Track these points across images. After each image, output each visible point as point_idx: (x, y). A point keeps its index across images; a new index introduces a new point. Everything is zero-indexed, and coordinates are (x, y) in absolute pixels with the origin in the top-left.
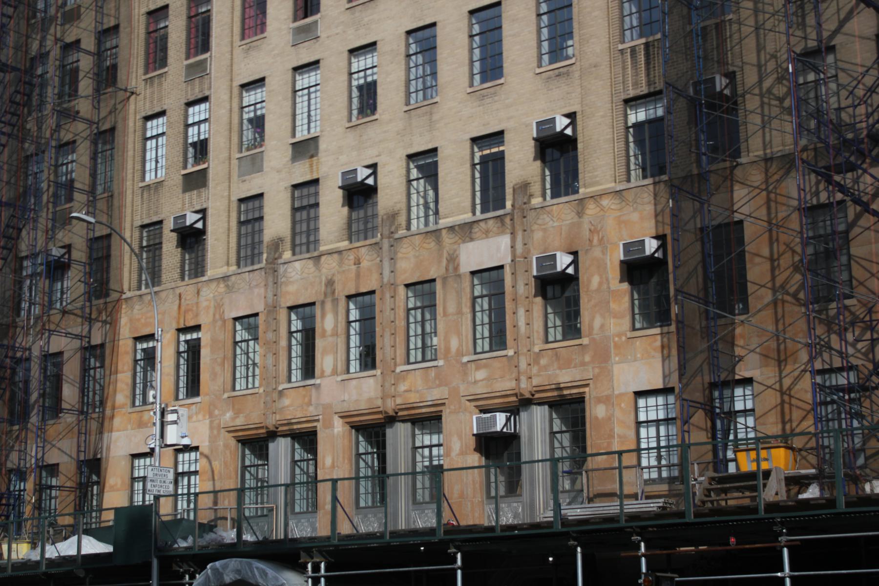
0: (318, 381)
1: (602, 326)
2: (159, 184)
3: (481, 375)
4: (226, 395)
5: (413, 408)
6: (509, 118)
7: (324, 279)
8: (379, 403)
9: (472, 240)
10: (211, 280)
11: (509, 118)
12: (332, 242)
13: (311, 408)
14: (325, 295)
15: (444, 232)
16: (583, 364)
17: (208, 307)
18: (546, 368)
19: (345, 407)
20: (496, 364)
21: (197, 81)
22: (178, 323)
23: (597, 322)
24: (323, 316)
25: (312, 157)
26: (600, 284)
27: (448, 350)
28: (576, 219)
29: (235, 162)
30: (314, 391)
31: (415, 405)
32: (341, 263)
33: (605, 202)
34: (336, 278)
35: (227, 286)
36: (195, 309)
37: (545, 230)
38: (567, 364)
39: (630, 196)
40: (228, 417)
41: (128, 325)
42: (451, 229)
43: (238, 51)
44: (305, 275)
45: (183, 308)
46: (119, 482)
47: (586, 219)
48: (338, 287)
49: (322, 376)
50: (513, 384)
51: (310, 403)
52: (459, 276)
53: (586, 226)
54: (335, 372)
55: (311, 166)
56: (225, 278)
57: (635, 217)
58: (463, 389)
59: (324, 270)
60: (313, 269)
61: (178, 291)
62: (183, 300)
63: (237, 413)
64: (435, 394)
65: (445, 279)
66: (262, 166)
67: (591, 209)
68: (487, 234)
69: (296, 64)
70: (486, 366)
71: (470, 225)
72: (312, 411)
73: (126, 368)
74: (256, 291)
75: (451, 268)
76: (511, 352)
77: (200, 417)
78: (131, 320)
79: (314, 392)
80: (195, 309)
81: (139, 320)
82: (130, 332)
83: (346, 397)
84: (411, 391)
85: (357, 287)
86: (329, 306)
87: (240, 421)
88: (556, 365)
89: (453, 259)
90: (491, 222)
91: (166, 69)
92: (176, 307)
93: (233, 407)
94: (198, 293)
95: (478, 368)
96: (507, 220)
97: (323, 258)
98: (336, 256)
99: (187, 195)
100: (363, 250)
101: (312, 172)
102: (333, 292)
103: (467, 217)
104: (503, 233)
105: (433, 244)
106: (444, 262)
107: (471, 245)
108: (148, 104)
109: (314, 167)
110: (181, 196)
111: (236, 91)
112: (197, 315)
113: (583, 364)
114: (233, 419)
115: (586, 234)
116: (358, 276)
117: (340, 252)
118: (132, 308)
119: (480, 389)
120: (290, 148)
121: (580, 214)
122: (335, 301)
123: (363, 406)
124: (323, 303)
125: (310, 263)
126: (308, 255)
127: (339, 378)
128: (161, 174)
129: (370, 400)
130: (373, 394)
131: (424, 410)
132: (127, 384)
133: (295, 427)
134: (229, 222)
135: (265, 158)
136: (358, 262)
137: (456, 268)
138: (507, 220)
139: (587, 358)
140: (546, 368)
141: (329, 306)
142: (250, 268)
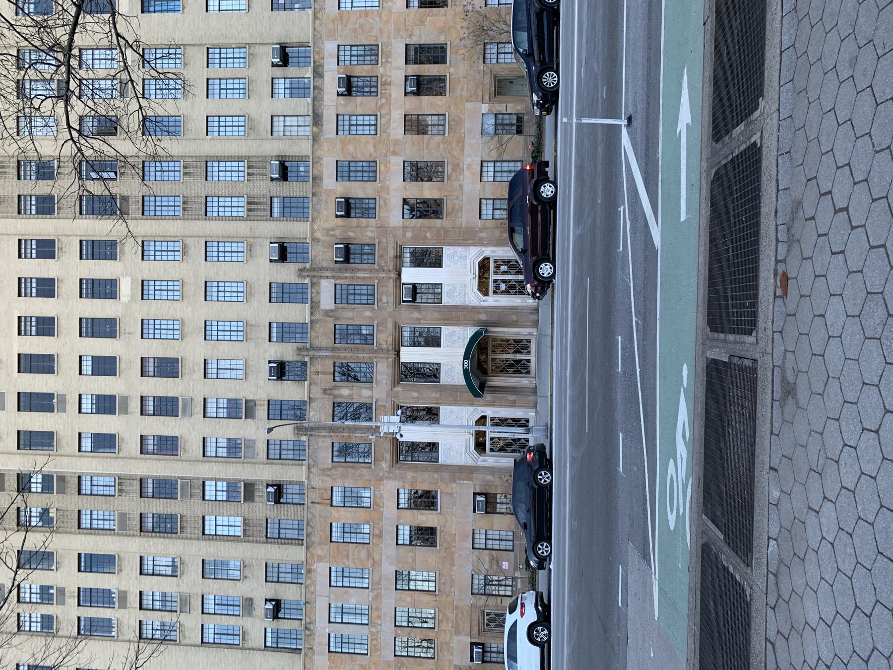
0: (374, 400)
1: (371, 232)
2: (245, 521)
3: (384, 299)
6: (265, 279)
9: (319, 302)
10: (308, 478)
11: (265, 279)
12: (304, 392)
13: (387, 406)
14: (331, 394)
15: (313, 318)
16: (387, 243)
17: (323, 481)
18: (386, 262)
19: (389, 383)
20: (381, 289)
21: (193, 491)
22: (327, 504)
23: (369, 234)
24: (341, 396)
25: (255, 404)
26: (352, 231)
27: (371, 317)
28: (321, 243)
29: (246, 460)
30: (379, 403)
32: (316, 384)
33: (316, 227)
34: (323, 387)
35: (314, 466)
36: (322, 491)
37: (323, 260)
38: (386, 250)
39: (315, 214)
40: (385, 465)
41: (323, 546)
42: (312, 314)
43: (183, 457)
44: (318, 410)
45: (320, 501)
46: (411, 554)
47: (322, 238)
48: (328, 386)
49: (371, 397)
50: (391, 280)
51: (385, 406)
52: (336, 309)
54: (371, 389)
55: (260, 405)
56: (309, 468)
57: (325, 213)
58: (390, 309)
59: (318, 396)
60: (316, 403)
61: (310, 504)
62: (316, 501)
63: (383, 458)
65: (337, 318)
66: (252, 440)
67: (318, 235)
68: (318, 293)
69: (202, 415)
70: (381, 296)
71: (312, 307)
73: (347, 548)
74: (320, 444)
75: (331, 314)
76: (376, 281)
77: (382, 487)
78: (320, 544)
79: (379, 403)
80: (322, 491)
81: (321, 537)
82: (326, 545)
83: (385, 382)
85: (329, 373)
86: (336, 392)
87: (388, 456)
88: (385, 257)
89: (327, 313)
90: (313, 290)
91: (179, 515)
92: (318, 506)
93: (380, 461)
94: (313, 488)
95: (381, 300)
96: (314, 280)
97: (312, 396)
98: (312, 387)
99: (256, 499)
100: (312, 369)
101: (263, 405)
102: (330, 389)
103: (308, 306)
104: (319, 284)
105: (317, 325)
106: (327, 318)
107: (322, 303)
108: (196, 532)
109: (261, 403)
110: (256, 504)
111: (205, 459)
112: (326, 489)
113: (387, 243)
114: (386, 461)
115: (328, 238)
116: (324, 373)
117: (310, 384)
118: (313, 542)
119: (391, 300)
120: (249, 420)
121: (318, 241)
122: (335, 387)
123: (390, 371)
124: (335, 396)
125: (312, 404)
126: (308, 406)
127: (375, 386)
128: (239, 521)
129: (388, 367)
130: (385, 365)
132: (356, 547)
134: (278, 464)
135: (248, 437)
136: (317, 373)
137: (331, 311)
138: (314, 280)
139: (385, 240)
140: (386, 262)
141: (336, 392)
142: (307, 447)
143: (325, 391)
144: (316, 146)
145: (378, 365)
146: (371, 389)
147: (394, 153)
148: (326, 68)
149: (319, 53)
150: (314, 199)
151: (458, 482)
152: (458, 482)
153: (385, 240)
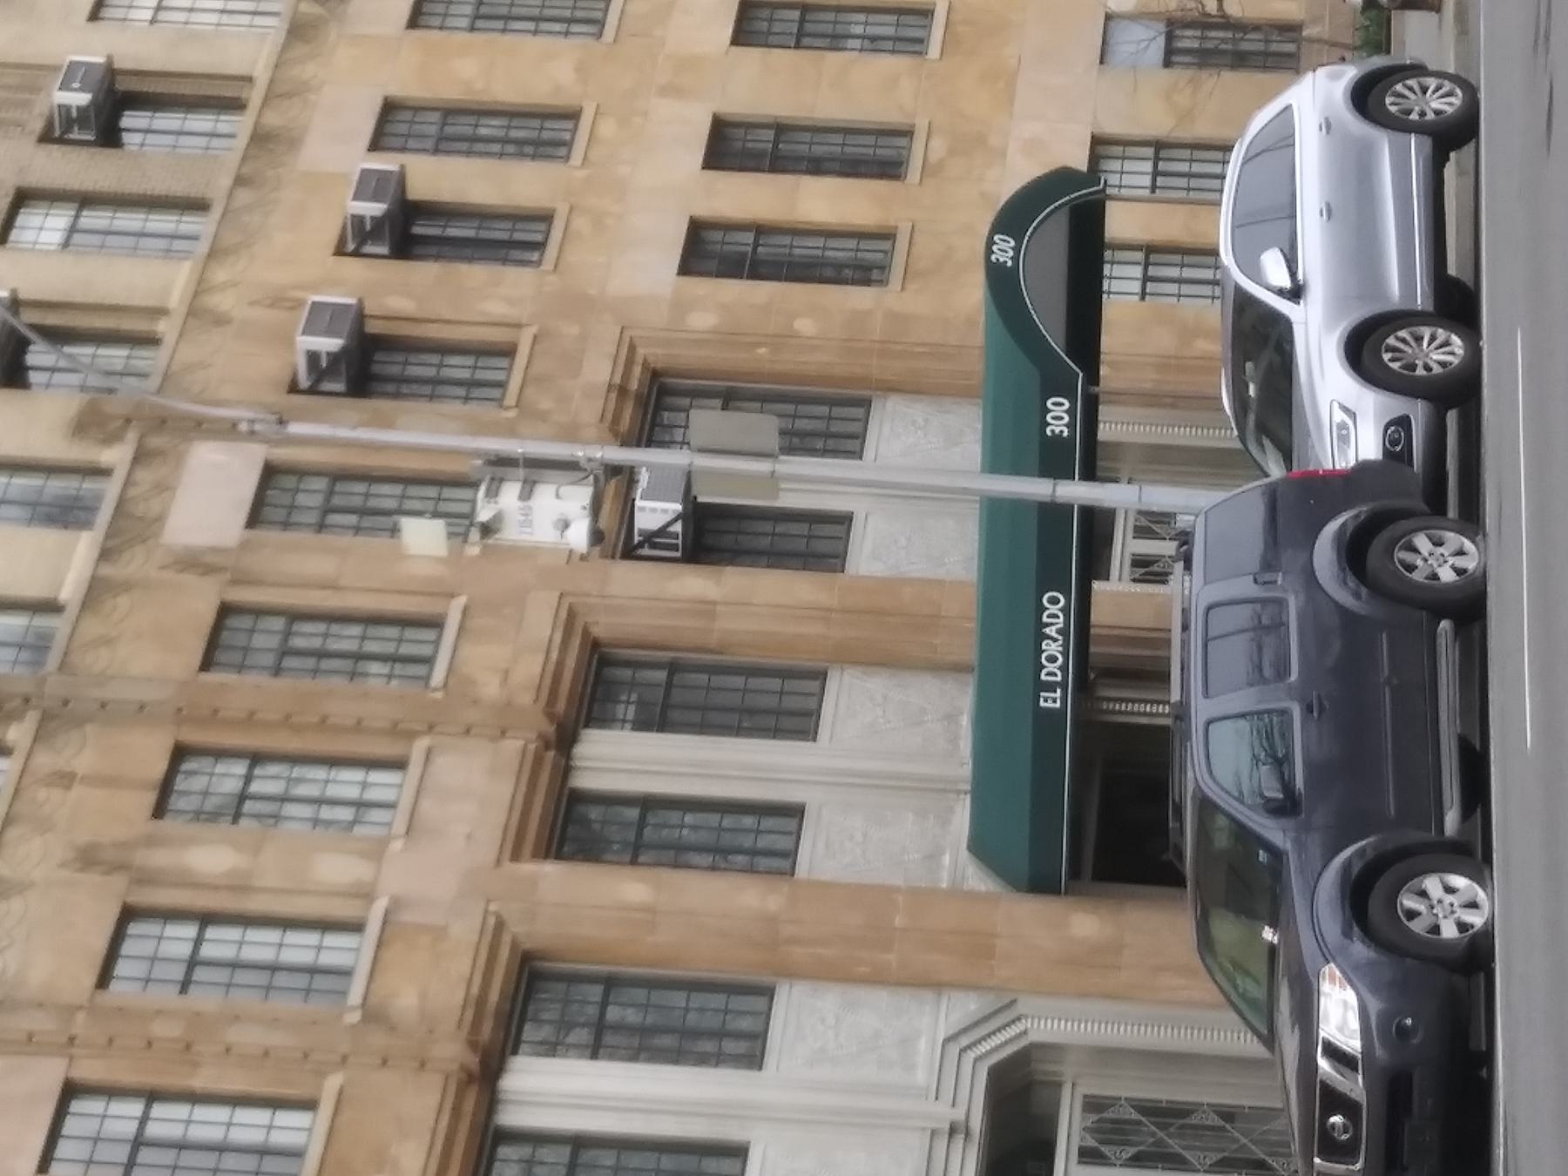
0: (380, 905)
7: (65, 874)
8: (512, 746)
9: (160, 519)
15: (107, 570)
30: (407, 917)
31: (551, 667)
32: (44, 826)
34: (83, 837)
51: (439, 933)
53: (259, 313)
64: (541, 622)
67: (222, 302)
68: (165, 488)
72: (465, 931)
79: (407, 917)
84: (506, 673)
86: (160, 858)
89: (193, 562)
105: (123, 601)
106: (189, 579)
122: (151, 841)
124: (145, 878)
131: (571, 663)
133: (494, 996)
136: (66, 779)
143: (88, 858)
144: (300, 50)
145: (441, 762)
146: (376, 851)
147: (672, 91)
150: (244, 196)
153: (573, 330)
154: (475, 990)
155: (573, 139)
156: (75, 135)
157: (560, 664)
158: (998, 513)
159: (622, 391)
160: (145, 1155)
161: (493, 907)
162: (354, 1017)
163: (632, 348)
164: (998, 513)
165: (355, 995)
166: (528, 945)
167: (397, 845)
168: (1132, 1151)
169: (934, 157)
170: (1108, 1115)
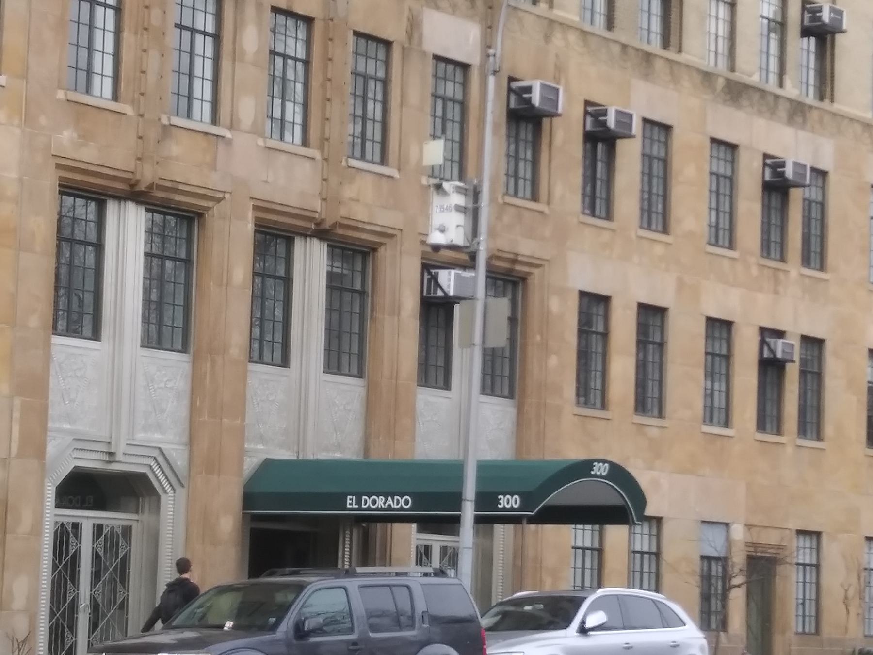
0: (228, 134)
4: (61, 95)
5: (356, 229)
8: (317, 205)
9: (437, 8)
30: (221, 147)
31: (360, 225)
51: (213, 167)
63: (85, 137)
64: (386, 219)
67: (558, 40)
72: (214, 181)
83: (270, 180)
84: (358, 201)
86: (250, 11)
89: (414, 25)
106: (405, 23)
122: (259, 6)
131: (364, 236)
133: (178, 198)
144: (697, 78)
145: (308, 164)
146: (256, 131)
147: (681, 285)
148: (802, 134)
149: (821, 121)
150: (616, 49)
151: (17, 401)
152: (17, 401)
154: (181, 187)
155: (770, 259)
156: (807, 16)
157: (363, 230)
158: (456, 470)
159: (514, 261)
160: (187, 34)
161: (227, 196)
162: (165, 121)
163: (538, 266)
164: (456, 470)
165: (176, 121)
166: (530, 281)
167: (260, 142)
168: (101, 553)
169: (647, 429)
170: (121, 541)
